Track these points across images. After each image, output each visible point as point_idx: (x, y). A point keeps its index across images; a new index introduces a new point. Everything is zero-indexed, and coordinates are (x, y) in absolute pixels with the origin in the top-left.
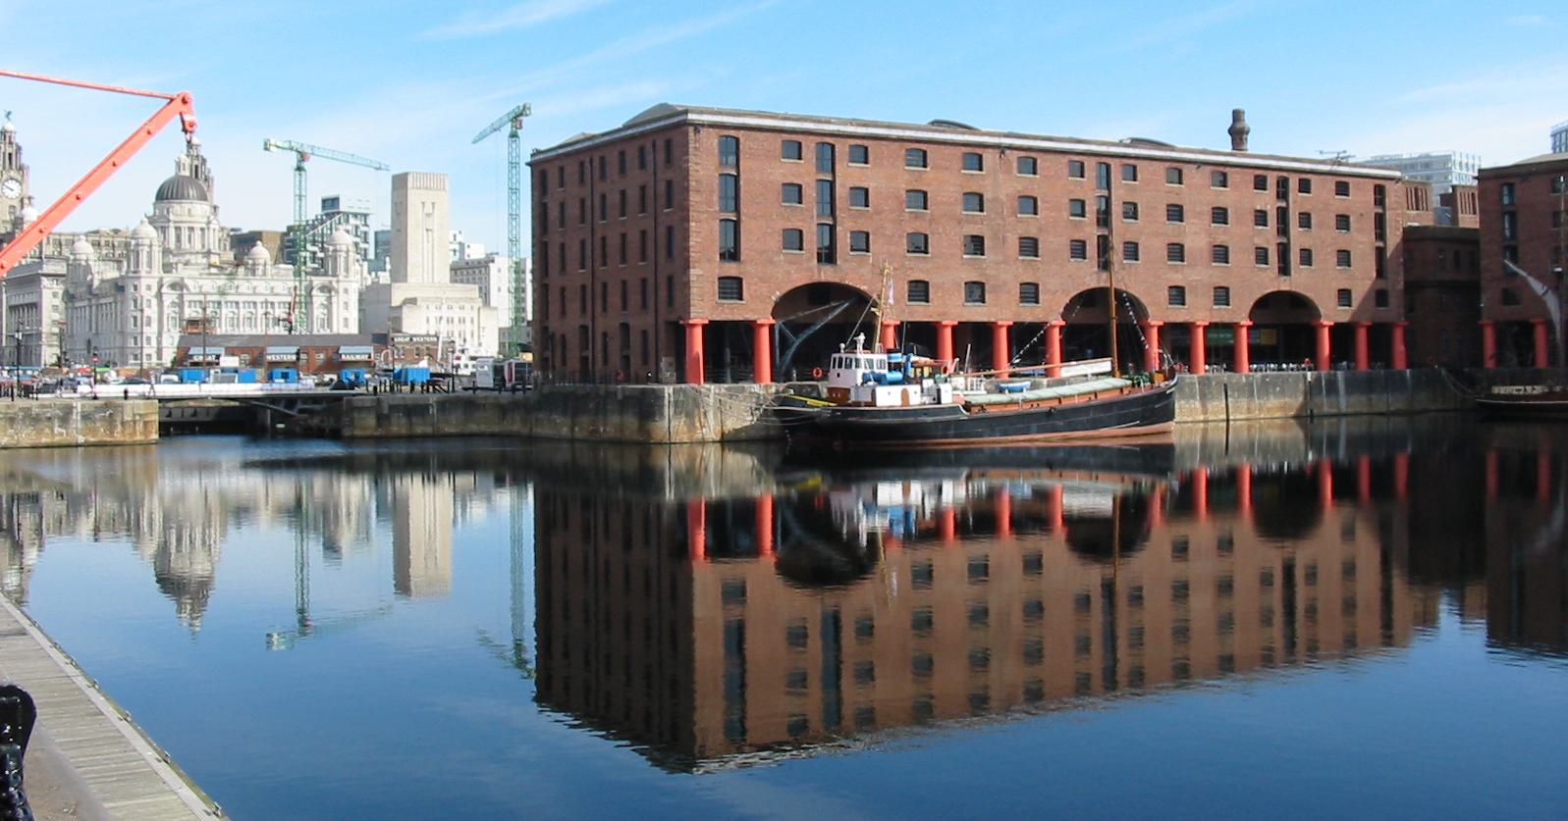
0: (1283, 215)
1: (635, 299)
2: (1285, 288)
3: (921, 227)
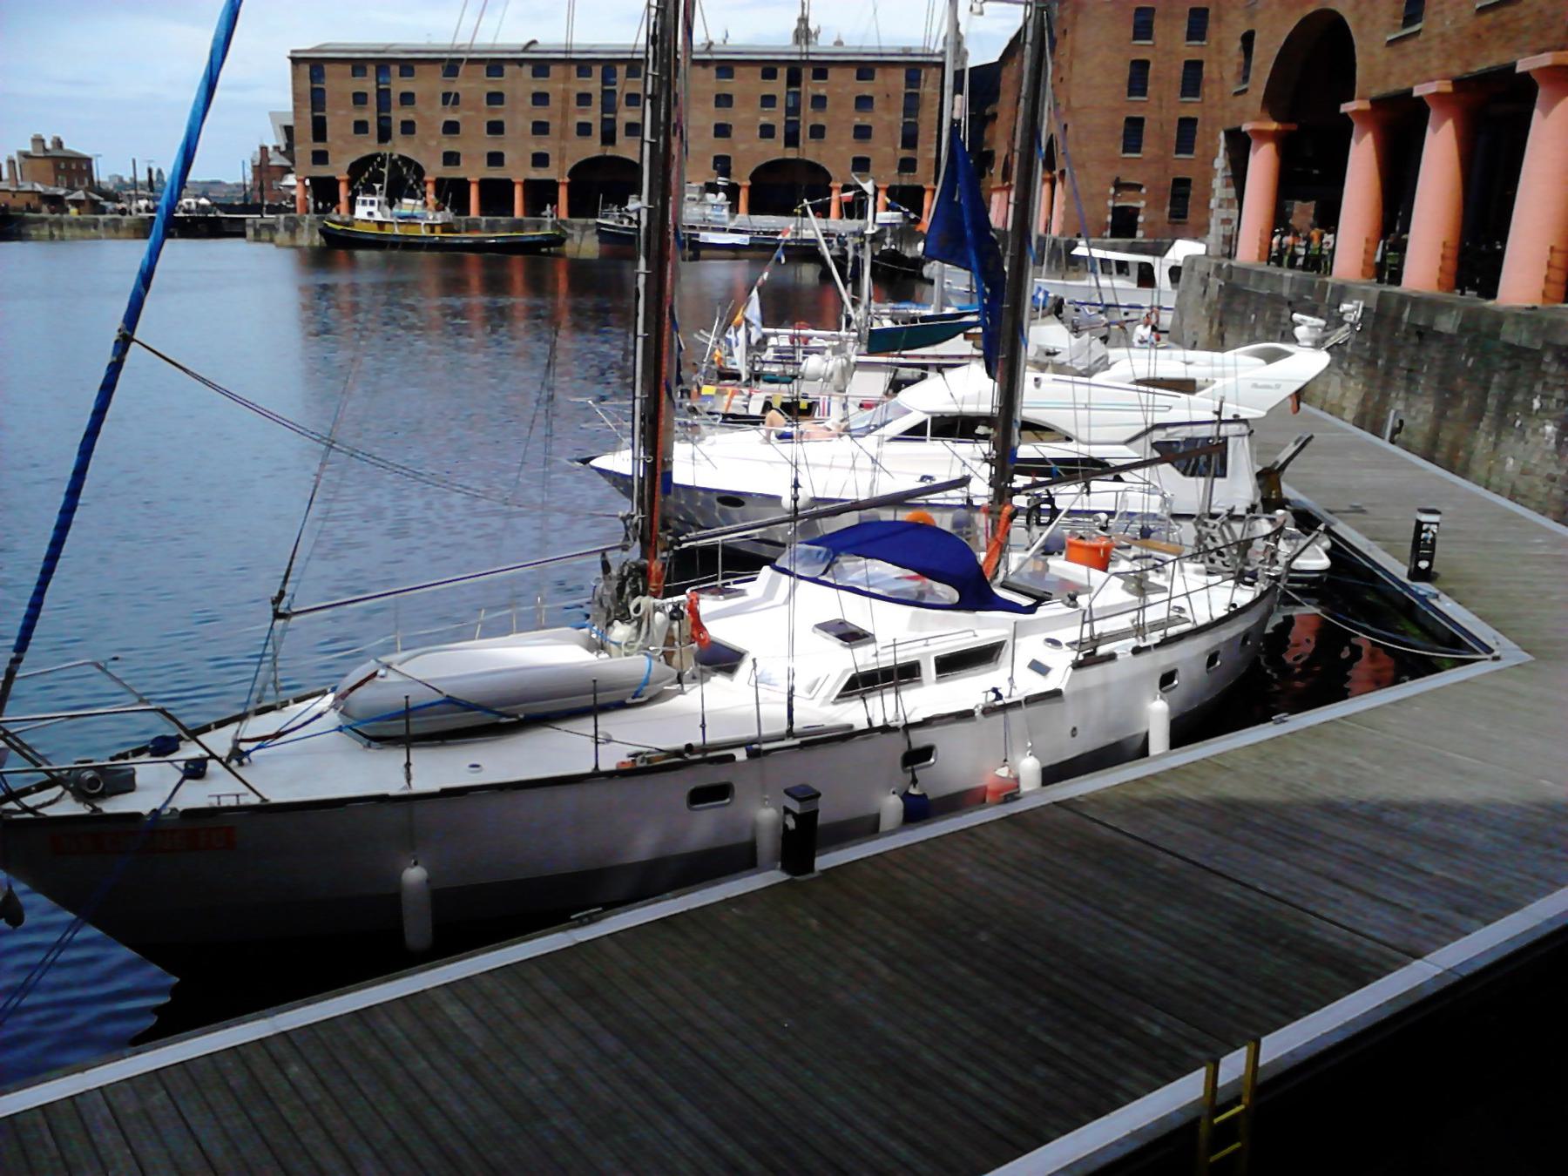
2: (789, 156)
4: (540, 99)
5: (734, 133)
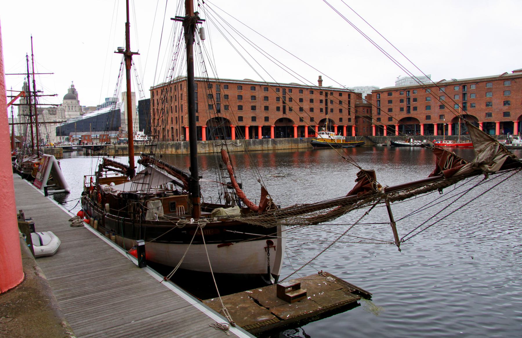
0: (326, 100)
1: (174, 121)
3: (241, 104)
4: (266, 98)
5: (314, 110)
